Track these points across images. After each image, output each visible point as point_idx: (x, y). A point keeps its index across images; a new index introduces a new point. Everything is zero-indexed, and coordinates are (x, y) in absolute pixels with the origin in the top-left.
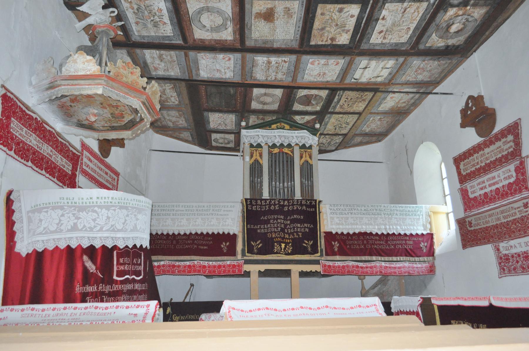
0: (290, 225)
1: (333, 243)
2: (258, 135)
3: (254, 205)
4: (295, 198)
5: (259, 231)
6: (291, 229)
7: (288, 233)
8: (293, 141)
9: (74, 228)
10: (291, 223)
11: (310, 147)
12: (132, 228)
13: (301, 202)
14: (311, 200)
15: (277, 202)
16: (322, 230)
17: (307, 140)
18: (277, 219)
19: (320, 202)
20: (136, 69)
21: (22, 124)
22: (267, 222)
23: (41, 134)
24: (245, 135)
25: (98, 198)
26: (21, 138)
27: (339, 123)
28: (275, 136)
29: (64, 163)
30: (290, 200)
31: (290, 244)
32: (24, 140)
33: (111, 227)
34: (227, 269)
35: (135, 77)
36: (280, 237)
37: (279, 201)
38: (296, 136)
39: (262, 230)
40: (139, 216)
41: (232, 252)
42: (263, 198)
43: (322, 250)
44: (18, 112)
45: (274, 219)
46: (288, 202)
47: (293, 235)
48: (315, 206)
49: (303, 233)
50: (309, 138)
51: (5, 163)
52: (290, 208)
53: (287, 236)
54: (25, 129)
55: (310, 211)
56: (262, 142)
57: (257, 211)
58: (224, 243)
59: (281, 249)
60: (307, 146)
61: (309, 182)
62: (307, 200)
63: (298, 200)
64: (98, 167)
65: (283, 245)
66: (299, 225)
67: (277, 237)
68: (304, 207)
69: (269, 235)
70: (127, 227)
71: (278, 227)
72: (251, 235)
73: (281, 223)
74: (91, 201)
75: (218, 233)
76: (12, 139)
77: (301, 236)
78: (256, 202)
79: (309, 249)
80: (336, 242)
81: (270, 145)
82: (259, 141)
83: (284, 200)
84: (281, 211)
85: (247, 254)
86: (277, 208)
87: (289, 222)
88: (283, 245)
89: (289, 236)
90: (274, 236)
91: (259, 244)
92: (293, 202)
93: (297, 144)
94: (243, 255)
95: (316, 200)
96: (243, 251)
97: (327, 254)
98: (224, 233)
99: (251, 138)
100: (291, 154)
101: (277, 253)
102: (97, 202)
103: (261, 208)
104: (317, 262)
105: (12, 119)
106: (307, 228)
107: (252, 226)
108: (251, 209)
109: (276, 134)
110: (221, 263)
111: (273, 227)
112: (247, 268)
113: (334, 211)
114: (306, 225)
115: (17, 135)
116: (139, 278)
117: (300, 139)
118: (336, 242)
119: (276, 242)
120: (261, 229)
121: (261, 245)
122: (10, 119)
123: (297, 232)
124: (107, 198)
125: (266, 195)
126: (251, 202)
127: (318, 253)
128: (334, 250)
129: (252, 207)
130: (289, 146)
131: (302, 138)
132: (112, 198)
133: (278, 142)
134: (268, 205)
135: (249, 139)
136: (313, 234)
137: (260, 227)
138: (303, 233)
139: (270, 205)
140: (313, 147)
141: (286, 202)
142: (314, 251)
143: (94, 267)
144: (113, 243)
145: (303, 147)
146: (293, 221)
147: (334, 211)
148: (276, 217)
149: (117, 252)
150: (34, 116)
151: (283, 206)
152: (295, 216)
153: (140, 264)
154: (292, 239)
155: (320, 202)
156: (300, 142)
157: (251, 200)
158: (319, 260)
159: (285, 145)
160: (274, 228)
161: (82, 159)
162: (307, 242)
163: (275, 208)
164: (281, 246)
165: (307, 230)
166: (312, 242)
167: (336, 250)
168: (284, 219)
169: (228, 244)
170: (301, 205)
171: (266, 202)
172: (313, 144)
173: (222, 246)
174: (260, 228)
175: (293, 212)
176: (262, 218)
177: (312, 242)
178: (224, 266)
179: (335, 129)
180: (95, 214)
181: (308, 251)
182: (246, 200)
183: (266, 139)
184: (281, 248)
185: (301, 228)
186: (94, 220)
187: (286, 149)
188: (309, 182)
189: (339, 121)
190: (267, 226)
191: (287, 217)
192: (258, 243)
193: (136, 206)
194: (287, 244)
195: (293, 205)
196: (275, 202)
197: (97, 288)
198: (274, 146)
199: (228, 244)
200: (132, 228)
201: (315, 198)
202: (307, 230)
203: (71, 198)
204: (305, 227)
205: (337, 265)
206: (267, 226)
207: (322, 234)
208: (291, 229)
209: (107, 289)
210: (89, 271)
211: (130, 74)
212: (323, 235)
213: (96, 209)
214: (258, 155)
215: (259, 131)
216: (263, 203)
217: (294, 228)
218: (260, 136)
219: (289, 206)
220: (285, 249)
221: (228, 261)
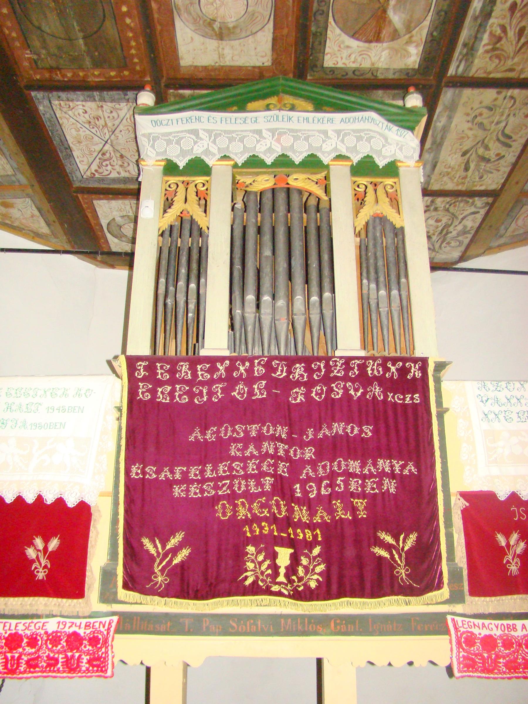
0: (313, 463)
1: (501, 539)
2: (195, 132)
3: (160, 383)
4: (338, 353)
5: (177, 491)
6: (319, 481)
7: (305, 501)
8: (328, 147)
10: (320, 455)
11: (392, 170)
13: (363, 368)
14: (404, 360)
15: (259, 370)
16: (455, 487)
17: (377, 143)
18: (259, 439)
19: (440, 366)
22: (216, 452)
24: (148, 136)
27: (481, 134)
28: (259, 132)
30: (318, 366)
31: (317, 551)
34: (44, 653)
36: (273, 519)
37: (269, 367)
38: (338, 132)
39: (194, 489)
41: (67, 580)
42: (203, 353)
43: (455, 575)
45: (247, 440)
46: (309, 370)
47: (331, 511)
48: (420, 386)
49: (372, 500)
50: (386, 139)
52: (317, 393)
53: (301, 514)
55: (397, 410)
56: (207, 152)
57: (172, 406)
58: (39, 542)
59: (276, 573)
60: (381, 163)
61: (395, 292)
62: (386, 360)
63: (348, 360)
65: (284, 556)
66: (354, 466)
67: (257, 519)
68: (377, 390)
69: (222, 512)
71: (262, 474)
72: (143, 508)
73: (275, 457)
75: (19, 500)
77: (362, 514)
78: (173, 372)
79: (402, 572)
80: (515, 537)
81: (240, 162)
82: (198, 151)
83: (290, 362)
84: (277, 407)
85: (122, 593)
86: (259, 391)
87: (309, 453)
88: (284, 556)
89: (312, 513)
90: (242, 513)
91: (175, 551)
92: (327, 366)
93: (340, 157)
94: (108, 596)
95: (424, 362)
96: (108, 575)
97: (478, 589)
98: (40, 498)
99: (169, 142)
100: (319, 192)
101: (254, 590)
103: (191, 394)
104: (435, 625)
106: (392, 476)
107: (151, 469)
108: (148, 397)
109: (262, 125)
110: (21, 627)
111: (237, 478)
112: (128, 649)
113: (496, 409)
114: (383, 464)
117: (351, 141)
118: (515, 537)
119: (255, 541)
120: (188, 483)
121: (185, 553)
123: (347, 496)
125: (216, 341)
126: (151, 368)
127: (439, 586)
128: (504, 569)
129: (153, 392)
130: (312, 163)
131: (359, 139)
133: (270, 150)
134: (220, 380)
135: (161, 145)
136: (415, 505)
137: (185, 475)
138: (372, 500)
139: (231, 381)
140: (401, 171)
141: (299, 370)
142: (424, 575)
145: (365, 167)
146: (330, 449)
147: (496, 409)
148: (254, 430)
151: (288, 385)
152: (338, 428)
154: (323, 526)
155: (440, 366)
156: (354, 149)
157: (151, 362)
158: (443, 615)
159: (297, 159)
160: (246, 477)
162: (389, 539)
163: (251, 393)
164: (274, 556)
165: (390, 486)
166: (413, 537)
167: (514, 568)
168: (290, 442)
169: (54, 544)
170: (364, 379)
171: (213, 370)
172: (399, 156)
173: (31, 553)
174: (186, 480)
175: (331, 410)
176: (196, 435)
177: (413, 537)
178: (33, 641)
179: (466, 169)
181: (393, 578)
182: (132, 362)
183: (223, 142)
184: (275, 568)
185: (364, 477)
187: (301, 176)
188: (395, 292)
189: (481, 125)
190: (215, 469)
191: (302, 432)
192: (173, 542)
194: (299, 548)
195: (327, 380)
196: (250, 371)
198: (254, 163)
199: (54, 544)
201: (418, 354)
202: (390, 486)
204: (382, 474)
205: (519, 633)
206: (215, 469)
207: (453, 499)
208: (319, 481)
212: (458, 505)
214: (192, 196)
215: (199, 119)
216: (203, 375)
217: (332, 476)
218: (202, 134)
219: (310, 384)
220: (291, 570)
221: (50, 615)
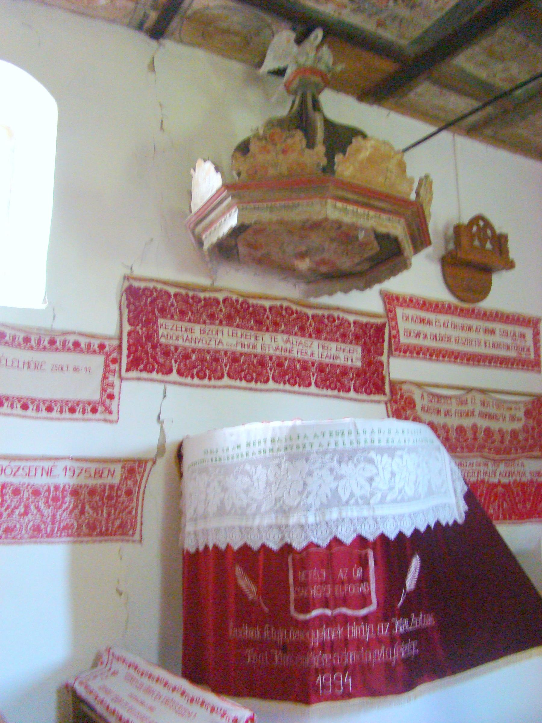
9: (221, 511)
12: (324, 500)
20: (292, 136)
21: (189, 321)
23: (249, 320)
25: (248, 444)
26: (193, 345)
29: (333, 352)
32: (200, 345)
33: (275, 504)
35: (293, 157)
40: (345, 469)
44: (172, 305)
51: (165, 396)
54: (197, 328)
64: (455, 327)
70: (310, 500)
74: (237, 451)
76: (167, 353)
102: (247, 454)
105: (161, 321)
115: (180, 342)
116: (363, 612)
122: (156, 322)
124: (263, 443)
132: (273, 441)
143: (254, 589)
144: (282, 539)
149: (293, 559)
150: (220, 297)
153: (365, 579)
161: (396, 327)
180: (247, 479)
186: (246, 491)
193: (332, 446)
197: (262, 633)
200: (324, 500)
203: (215, 450)
209: (281, 636)
210: (246, 596)
211: (281, 156)
213: (247, 467)
